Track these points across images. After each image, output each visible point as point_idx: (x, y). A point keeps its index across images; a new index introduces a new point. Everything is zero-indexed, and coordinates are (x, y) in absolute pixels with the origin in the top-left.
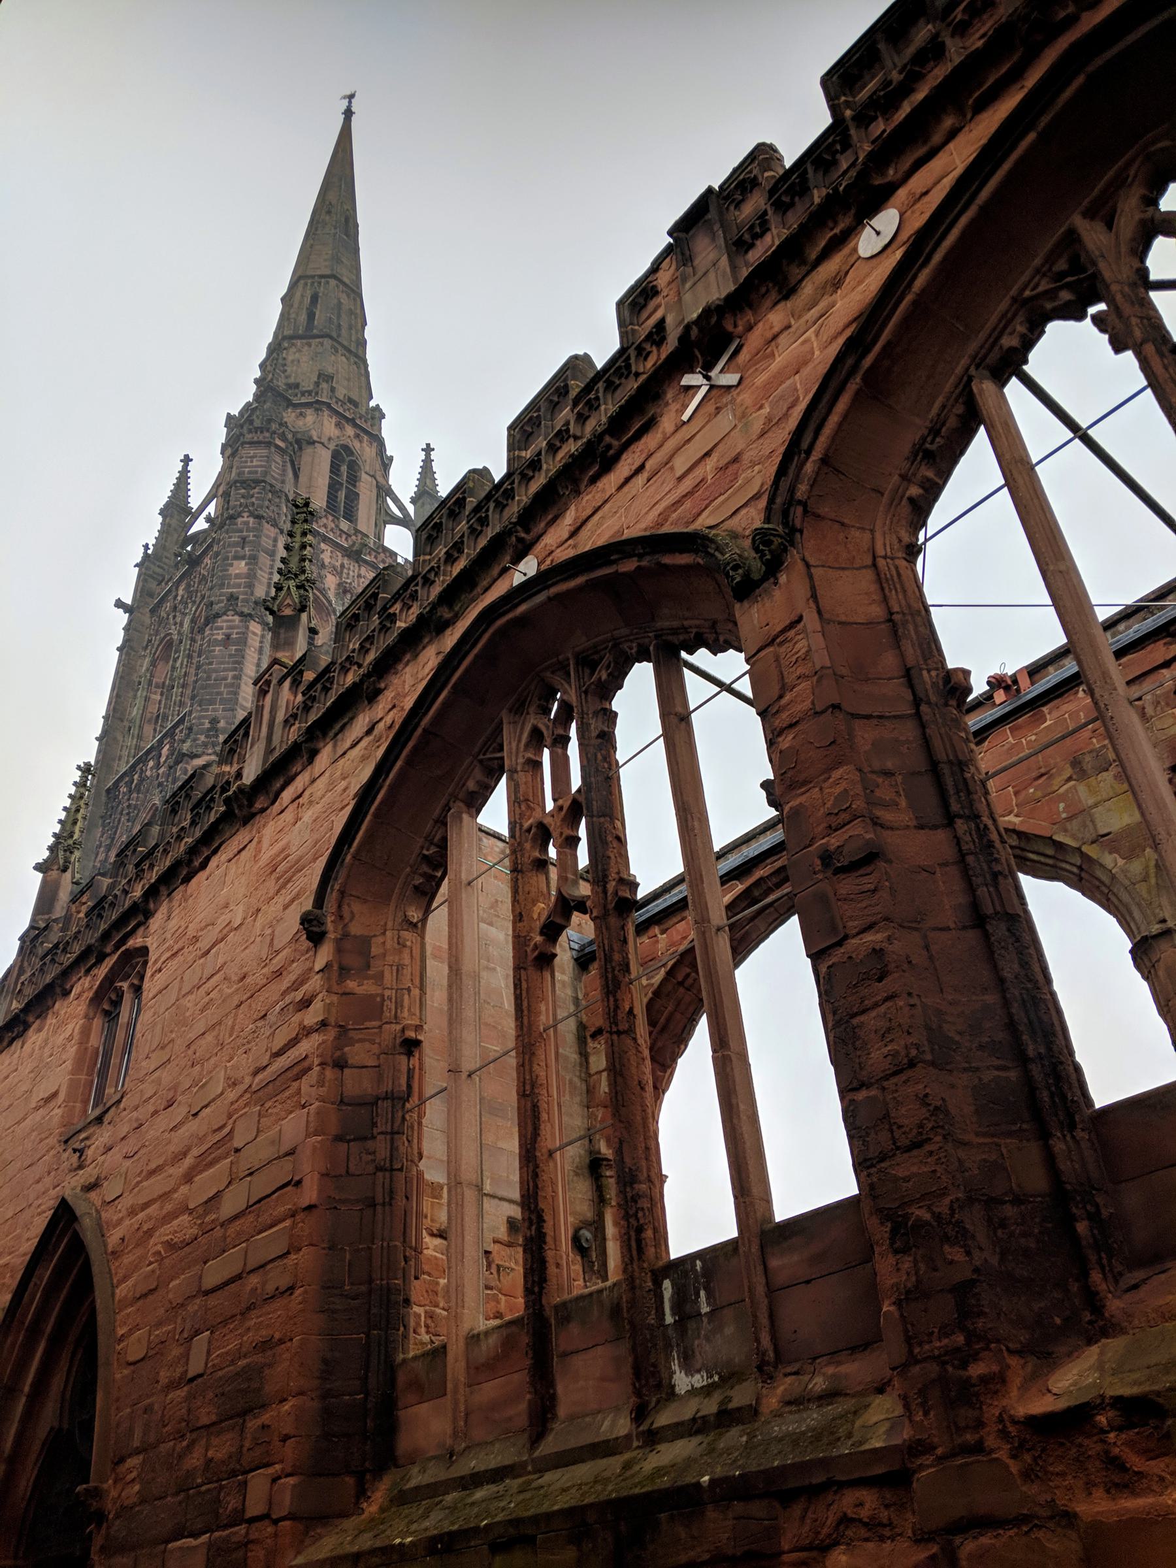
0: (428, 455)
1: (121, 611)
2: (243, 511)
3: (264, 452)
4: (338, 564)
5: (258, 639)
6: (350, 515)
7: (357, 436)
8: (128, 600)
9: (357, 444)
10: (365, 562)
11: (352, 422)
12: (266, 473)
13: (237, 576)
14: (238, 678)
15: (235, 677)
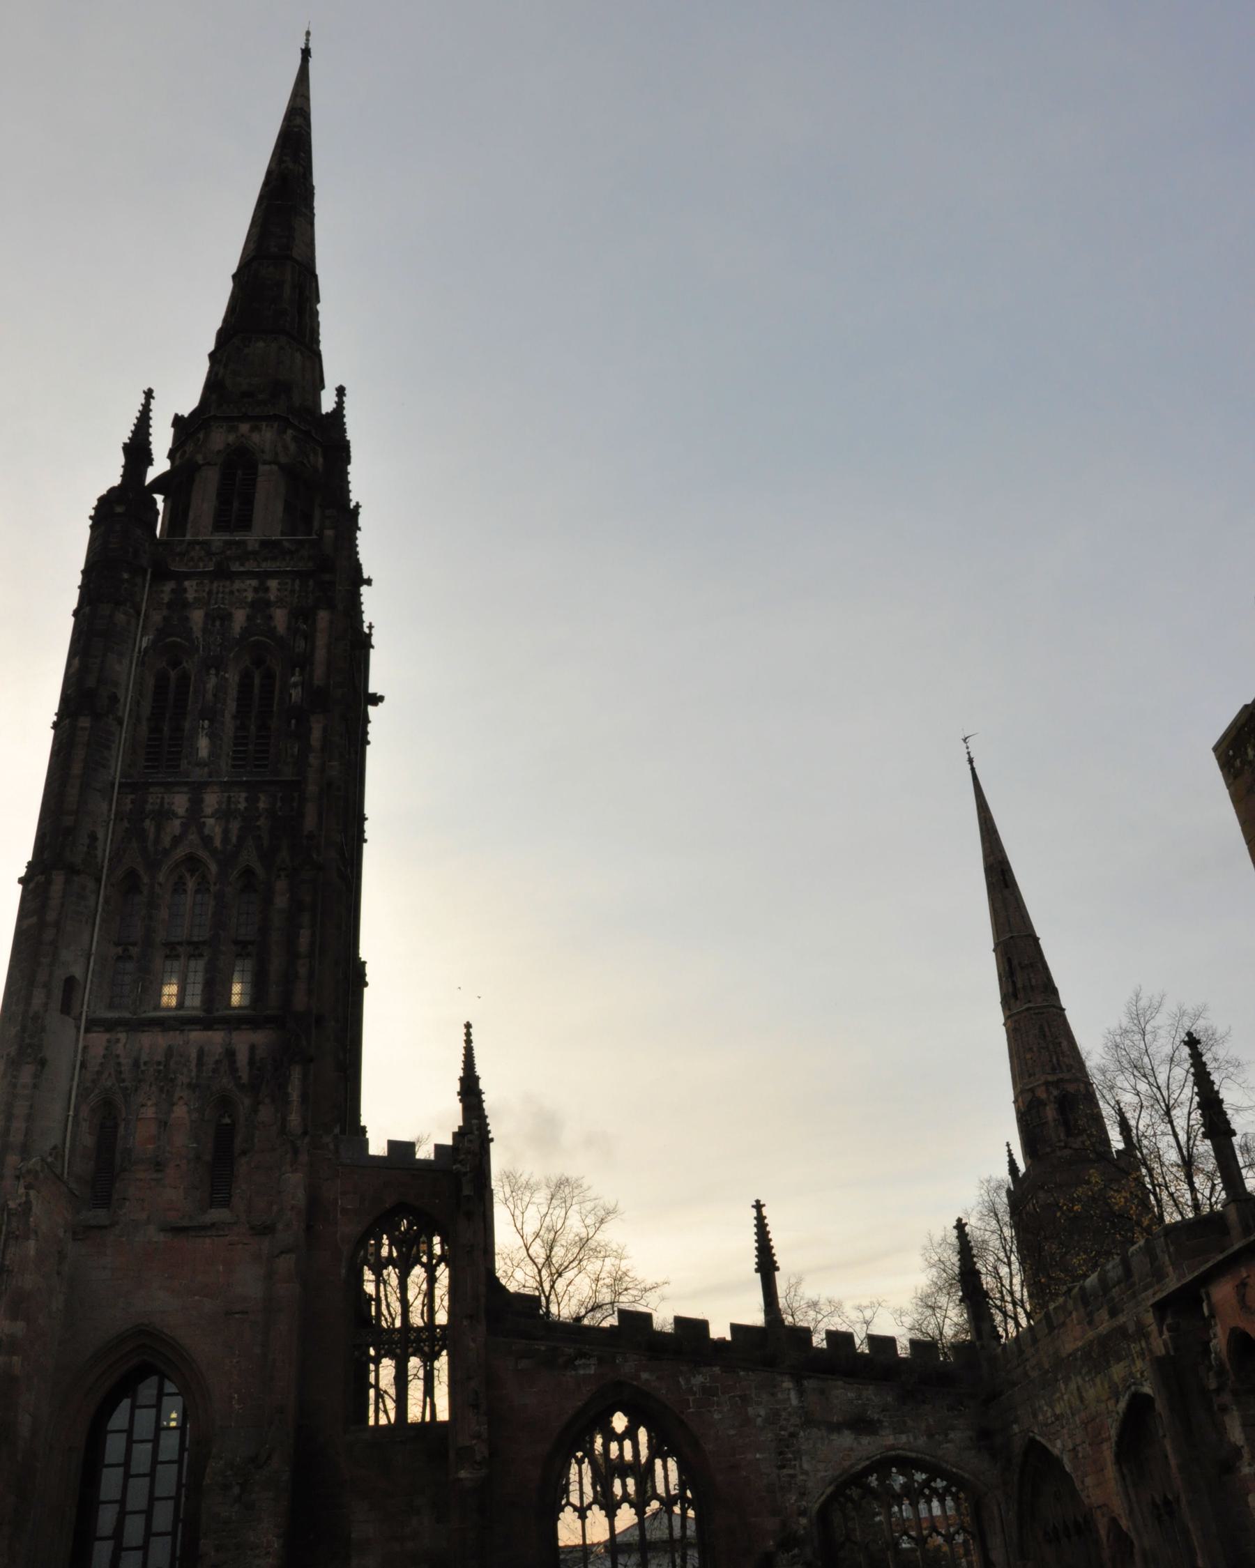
6: (245, 523)
7: (255, 429)
11: (245, 418)
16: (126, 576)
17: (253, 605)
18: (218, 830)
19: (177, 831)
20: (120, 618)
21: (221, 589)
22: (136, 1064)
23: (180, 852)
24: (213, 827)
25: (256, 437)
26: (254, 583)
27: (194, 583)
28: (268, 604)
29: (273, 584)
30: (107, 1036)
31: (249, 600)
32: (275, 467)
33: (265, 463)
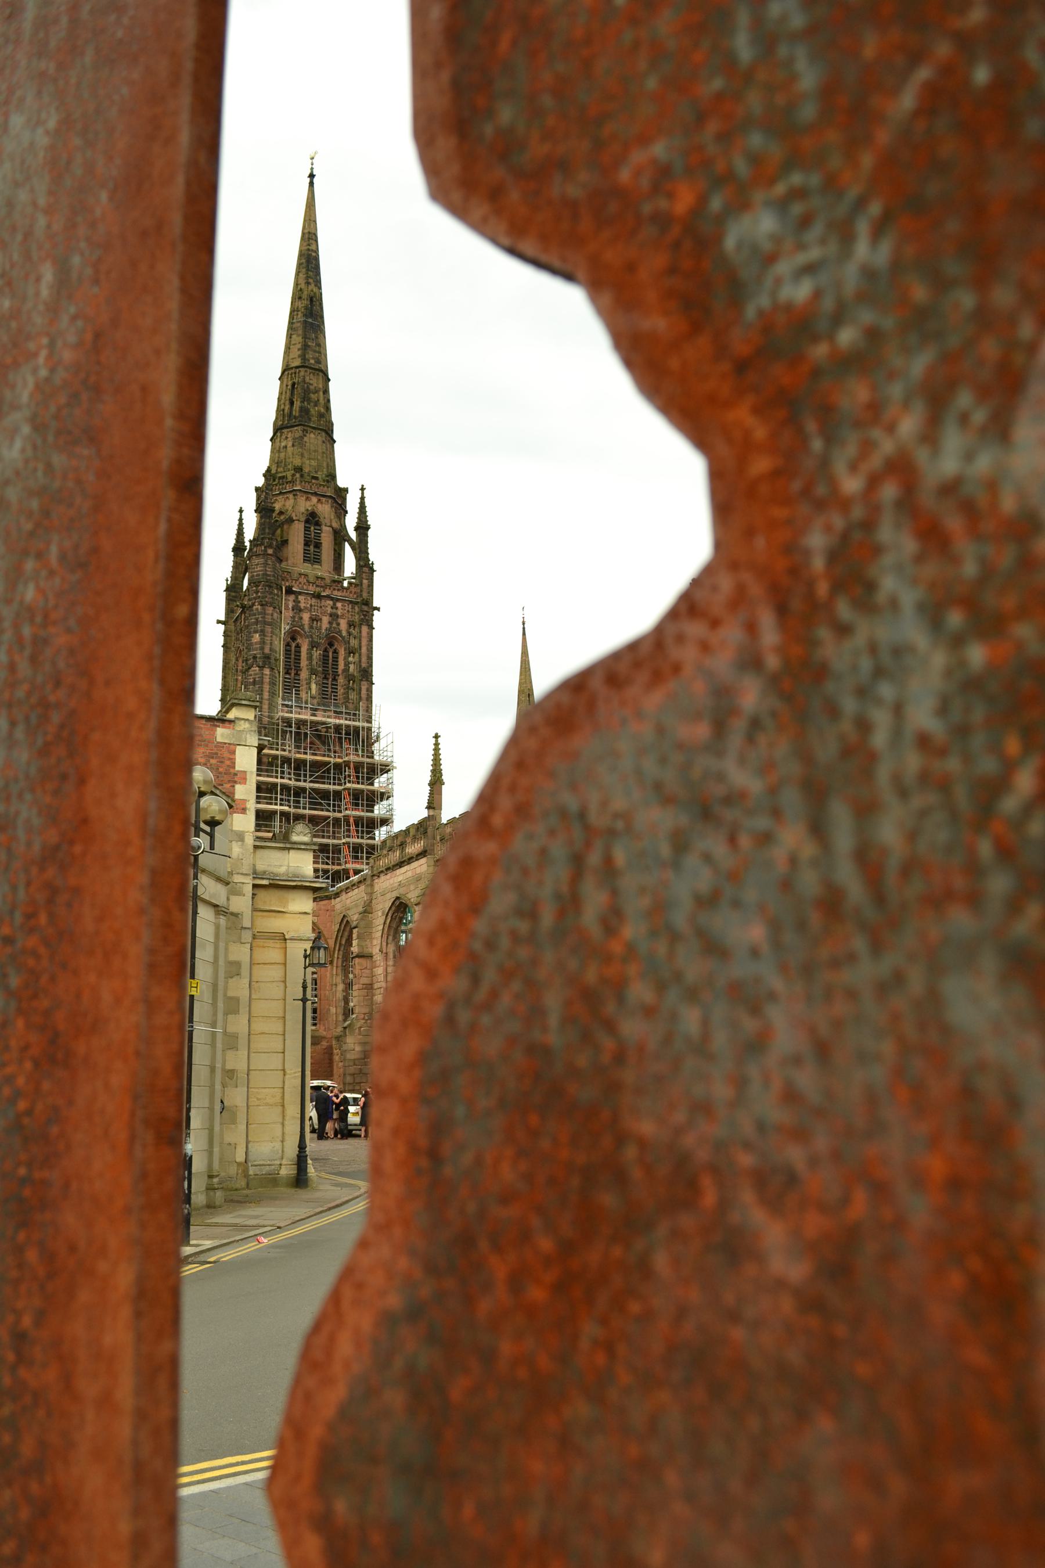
0: (363, 494)
1: (220, 624)
2: (255, 602)
3: (262, 561)
4: (308, 606)
5: (268, 677)
8: (223, 618)
9: (319, 506)
10: (324, 596)
11: (315, 494)
12: (263, 574)
13: (256, 643)
16: (276, 591)
20: (275, 615)
21: (316, 604)
26: (331, 603)
27: (303, 597)
28: (338, 616)
29: (339, 605)
31: (329, 612)
32: (331, 529)
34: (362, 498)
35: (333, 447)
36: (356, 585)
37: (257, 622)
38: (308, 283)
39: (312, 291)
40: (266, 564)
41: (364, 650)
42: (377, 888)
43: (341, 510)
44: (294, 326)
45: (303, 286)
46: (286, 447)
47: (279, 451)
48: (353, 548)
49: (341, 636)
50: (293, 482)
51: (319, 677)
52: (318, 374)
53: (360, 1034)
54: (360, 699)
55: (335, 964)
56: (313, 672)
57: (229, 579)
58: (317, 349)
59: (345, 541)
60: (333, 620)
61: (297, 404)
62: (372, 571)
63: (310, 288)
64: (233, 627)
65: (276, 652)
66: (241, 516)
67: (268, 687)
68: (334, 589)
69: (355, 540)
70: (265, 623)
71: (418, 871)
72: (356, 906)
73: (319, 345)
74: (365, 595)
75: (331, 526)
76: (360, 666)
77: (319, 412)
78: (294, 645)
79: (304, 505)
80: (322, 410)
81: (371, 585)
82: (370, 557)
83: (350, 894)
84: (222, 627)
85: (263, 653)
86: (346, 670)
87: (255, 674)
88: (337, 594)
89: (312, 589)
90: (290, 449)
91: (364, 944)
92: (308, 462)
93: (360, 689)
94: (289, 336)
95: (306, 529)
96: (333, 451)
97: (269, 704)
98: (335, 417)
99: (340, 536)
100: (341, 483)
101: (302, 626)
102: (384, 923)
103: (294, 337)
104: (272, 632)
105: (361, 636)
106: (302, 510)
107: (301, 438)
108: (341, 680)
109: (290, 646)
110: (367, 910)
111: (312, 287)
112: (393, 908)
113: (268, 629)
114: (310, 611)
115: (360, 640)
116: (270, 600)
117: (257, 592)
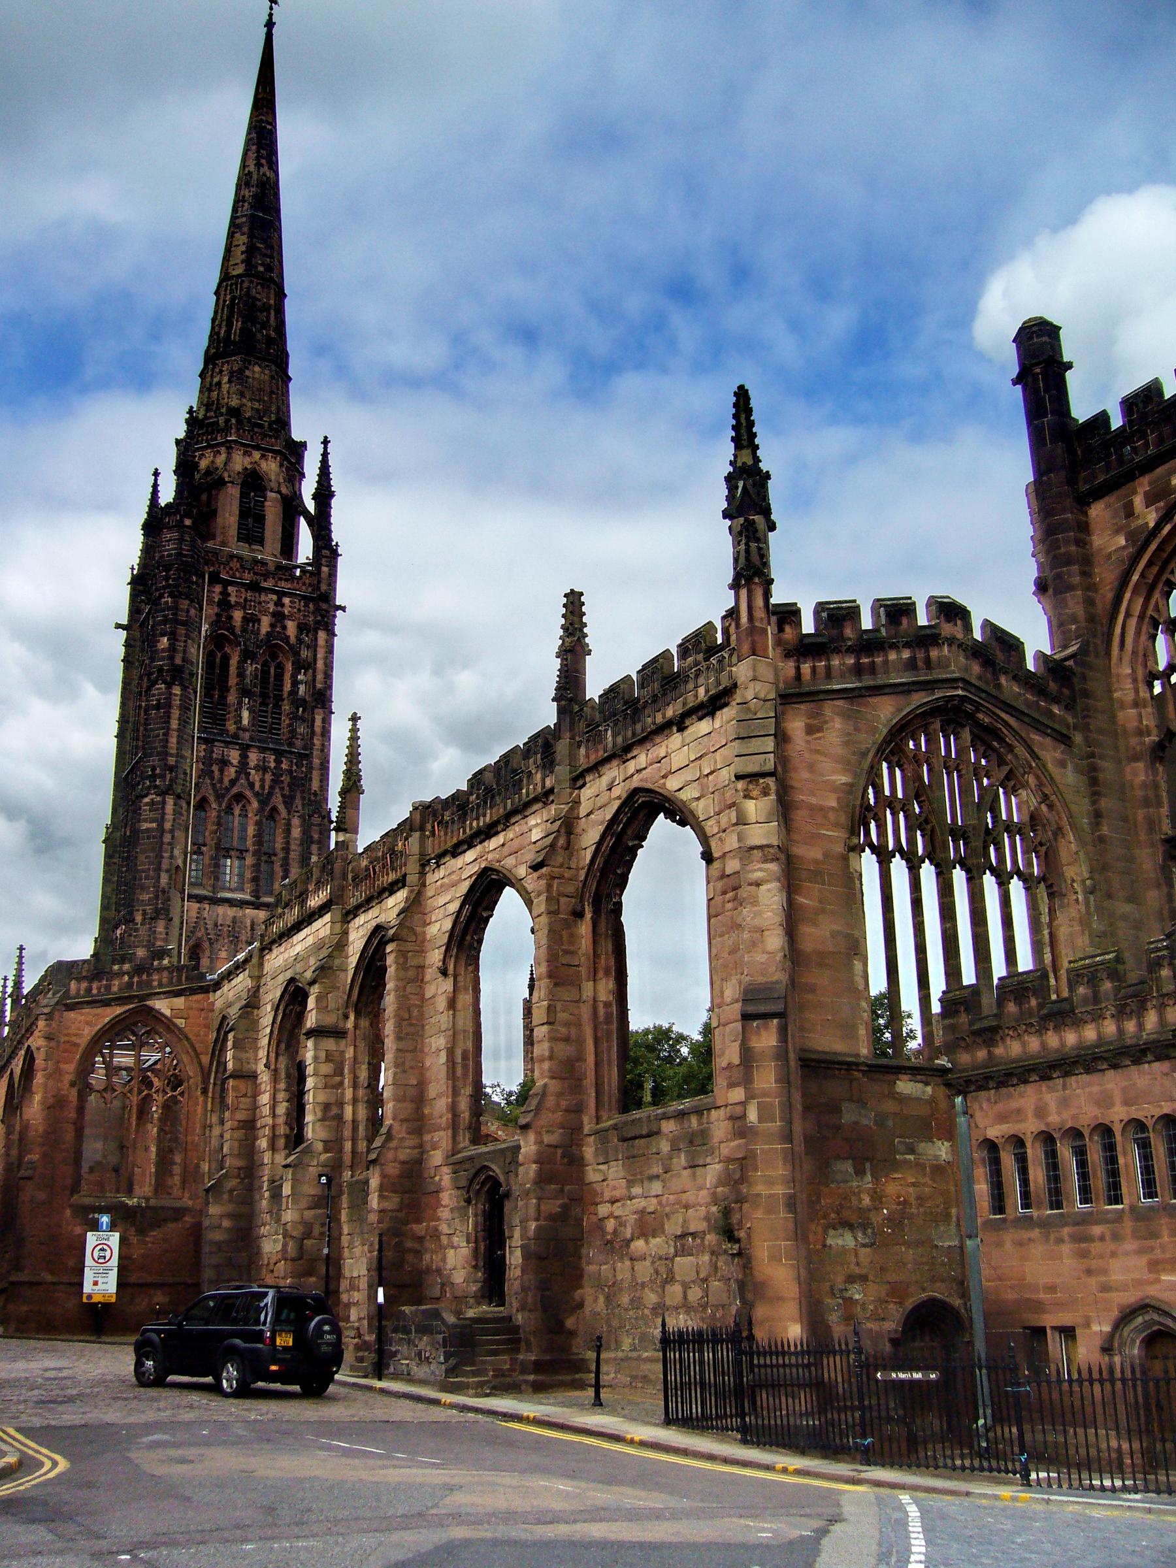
0: (325, 448)
7: (263, 456)
8: (124, 621)
11: (257, 448)
12: (178, 554)
13: (163, 650)
14: (166, 734)
15: (164, 734)
16: (194, 579)
17: (274, 614)
18: (257, 778)
19: (233, 776)
20: (193, 612)
22: (216, 925)
23: (235, 790)
24: (255, 776)
25: (264, 464)
26: (275, 597)
29: (286, 600)
30: (198, 905)
33: (271, 491)
34: (325, 455)
35: (287, 387)
36: (311, 573)
37: (164, 622)
38: (259, 165)
39: (264, 174)
40: (181, 540)
41: (320, 664)
42: (267, 967)
43: (295, 473)
44: (238, 221)
45: (252, 168)
46: (219, 384)
47: (210, 390)
48: (310, 524)
49: (288, 643)
50: (226, 430)
51: (255, 701)
52: (268, 287)
53: (230, 1201)
54: (313, 733)
55: (210, 1095)
56: (244, 692)
57: (136, 567)
58: (269, 252)
59: (300, 513)
60: (278, 621)
61: (237, 325)
62: (335, 554)
63: (262, 170)
64: (137, 634)
65: (192, 663)
66: (156, 480)
67: (178, 712)
68: (281, 579)
69: (313, 512)
70: (177, 622)
71: (322, 934)
72: (239, 998)
73: (271, 247)
74: (324, 587)
75: (279, 492)
76: (314, 686)
77: (268, 336)
78: (219, 655)
79: (240, 461)
80: (273, 334)
81: (333, 575)
82: (333, 536)
83: (234, 982)
84: (123, 634)
85: (173, 664)
86: (294, 692)
87: (160, 694)
88: (284, 586)
89: (247, 578)
90: (225, 387)
91: (244, 1056)
92: (249, 404)
93: (313, 721)
94: (231, 235)
95: (242, 495)
96: (288, 391)
97: (178, 736)
98: (291, 346)
99: (292, 507)
100: (297, 435)
101: (231, 629)
102: (274, 1022)
103: (237, 235)
104: (187, 636)
105: (316, 646)
106: (238, 468)
107: (241, 371)
108: (286, 707)
109: (215, 658)
110: (252, 1003)
111: (266, 169)
112: (287, 997)
113: (181, 630)
114: (244, 608)
115: (316, 651)
116: (185, 590)
117: (167, 578)
